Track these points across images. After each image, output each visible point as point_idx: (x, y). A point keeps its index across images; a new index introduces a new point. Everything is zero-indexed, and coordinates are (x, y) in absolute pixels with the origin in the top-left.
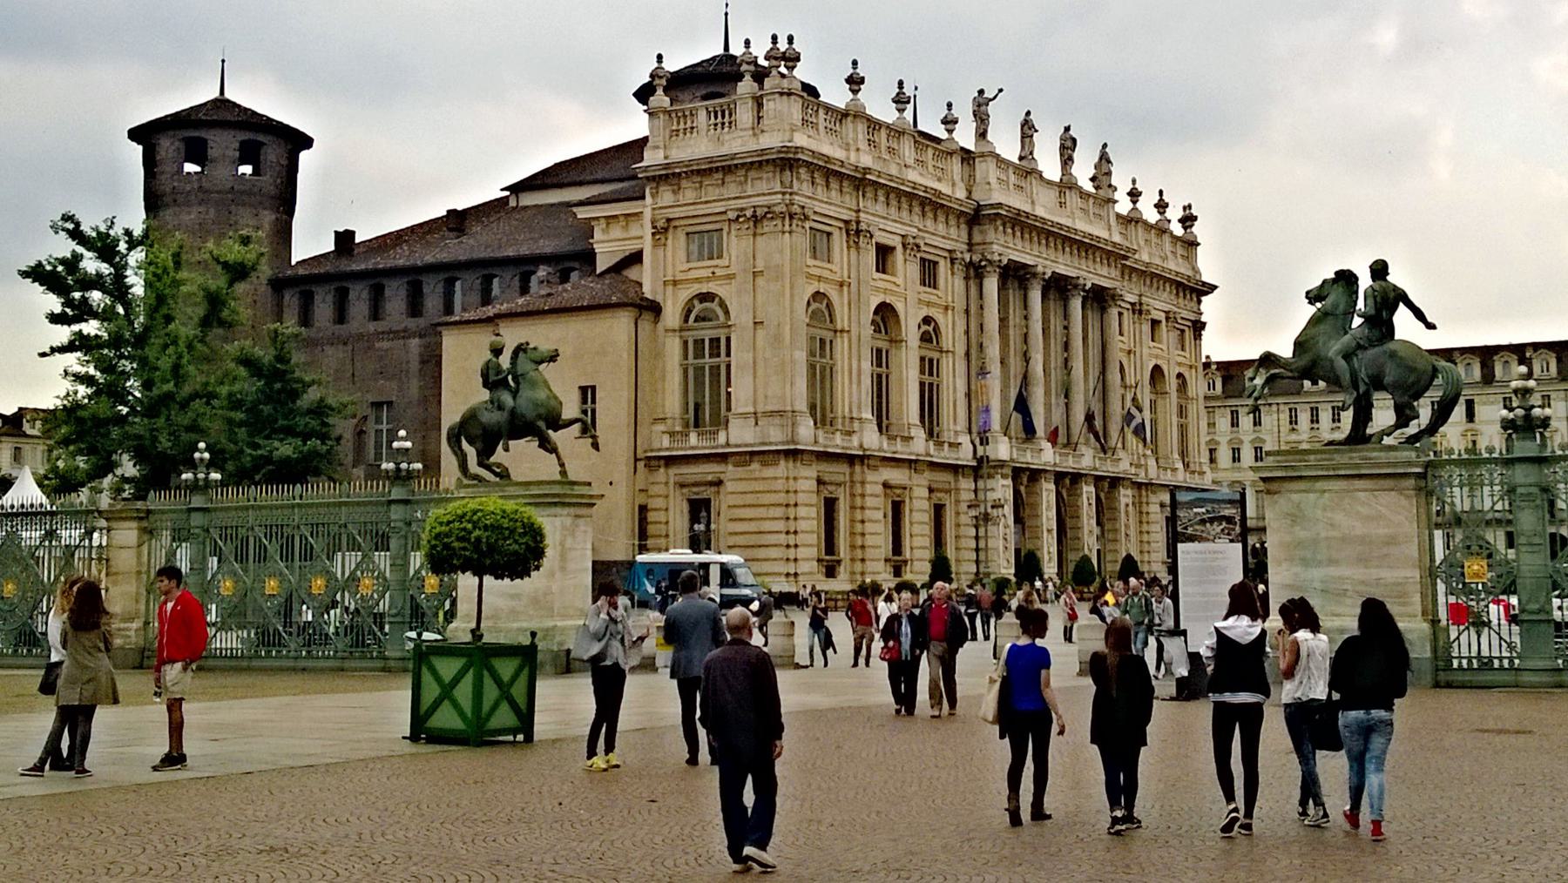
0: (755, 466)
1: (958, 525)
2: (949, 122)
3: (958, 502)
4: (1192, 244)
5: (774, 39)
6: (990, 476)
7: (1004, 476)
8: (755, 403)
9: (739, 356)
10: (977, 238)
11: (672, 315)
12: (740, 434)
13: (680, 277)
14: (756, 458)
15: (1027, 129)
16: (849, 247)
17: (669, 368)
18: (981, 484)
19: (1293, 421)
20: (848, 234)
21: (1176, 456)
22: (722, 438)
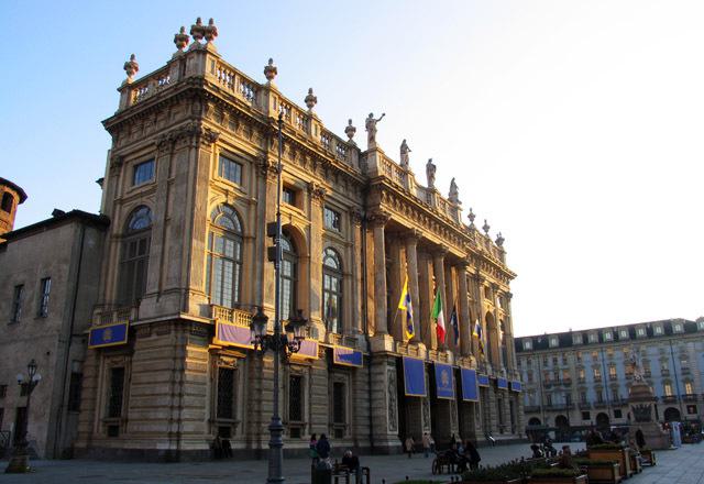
0: (154, 337)
1: (355, 399)
2: (350, 131)
3: (354, 381)
4: (502, 253)
5: (199, 21)
6: (381, 364)
7: (389, 364)
8: (160, 285)
9: (155, 249)
10: (370, 202)
11: (117, 227)
12: (148, 309)
13: (126, 196)
14: (156, 329)
15: (404, 149)
16: (257, 177)
17: (111, 264)
18: (374, 370)
19: (545, 363)
20: (257, 167)
21: (502, 364)
22: (133, 317)
